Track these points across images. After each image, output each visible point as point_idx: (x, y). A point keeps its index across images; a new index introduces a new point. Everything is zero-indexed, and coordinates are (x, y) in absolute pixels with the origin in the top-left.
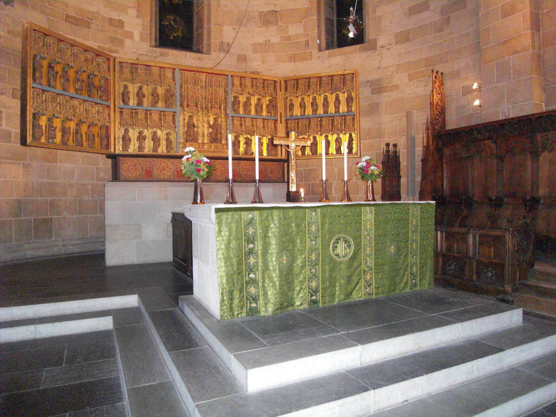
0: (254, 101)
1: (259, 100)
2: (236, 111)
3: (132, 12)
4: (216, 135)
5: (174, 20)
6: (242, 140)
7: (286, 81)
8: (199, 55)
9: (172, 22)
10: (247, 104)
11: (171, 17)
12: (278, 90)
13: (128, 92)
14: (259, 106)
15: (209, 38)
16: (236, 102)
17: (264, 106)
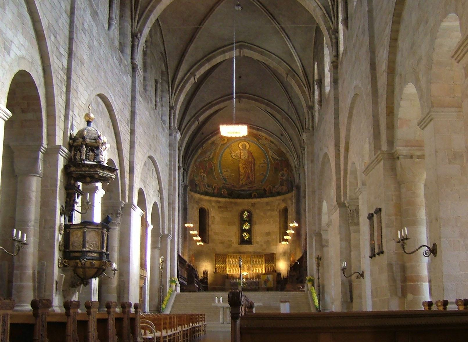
0: (258, 260)
2: (253, 263)
3: (234, 237)
5: (246, 234)
10: (256, 261)
11: (245, 233)
14: (259, 261)
16: (253, 260)
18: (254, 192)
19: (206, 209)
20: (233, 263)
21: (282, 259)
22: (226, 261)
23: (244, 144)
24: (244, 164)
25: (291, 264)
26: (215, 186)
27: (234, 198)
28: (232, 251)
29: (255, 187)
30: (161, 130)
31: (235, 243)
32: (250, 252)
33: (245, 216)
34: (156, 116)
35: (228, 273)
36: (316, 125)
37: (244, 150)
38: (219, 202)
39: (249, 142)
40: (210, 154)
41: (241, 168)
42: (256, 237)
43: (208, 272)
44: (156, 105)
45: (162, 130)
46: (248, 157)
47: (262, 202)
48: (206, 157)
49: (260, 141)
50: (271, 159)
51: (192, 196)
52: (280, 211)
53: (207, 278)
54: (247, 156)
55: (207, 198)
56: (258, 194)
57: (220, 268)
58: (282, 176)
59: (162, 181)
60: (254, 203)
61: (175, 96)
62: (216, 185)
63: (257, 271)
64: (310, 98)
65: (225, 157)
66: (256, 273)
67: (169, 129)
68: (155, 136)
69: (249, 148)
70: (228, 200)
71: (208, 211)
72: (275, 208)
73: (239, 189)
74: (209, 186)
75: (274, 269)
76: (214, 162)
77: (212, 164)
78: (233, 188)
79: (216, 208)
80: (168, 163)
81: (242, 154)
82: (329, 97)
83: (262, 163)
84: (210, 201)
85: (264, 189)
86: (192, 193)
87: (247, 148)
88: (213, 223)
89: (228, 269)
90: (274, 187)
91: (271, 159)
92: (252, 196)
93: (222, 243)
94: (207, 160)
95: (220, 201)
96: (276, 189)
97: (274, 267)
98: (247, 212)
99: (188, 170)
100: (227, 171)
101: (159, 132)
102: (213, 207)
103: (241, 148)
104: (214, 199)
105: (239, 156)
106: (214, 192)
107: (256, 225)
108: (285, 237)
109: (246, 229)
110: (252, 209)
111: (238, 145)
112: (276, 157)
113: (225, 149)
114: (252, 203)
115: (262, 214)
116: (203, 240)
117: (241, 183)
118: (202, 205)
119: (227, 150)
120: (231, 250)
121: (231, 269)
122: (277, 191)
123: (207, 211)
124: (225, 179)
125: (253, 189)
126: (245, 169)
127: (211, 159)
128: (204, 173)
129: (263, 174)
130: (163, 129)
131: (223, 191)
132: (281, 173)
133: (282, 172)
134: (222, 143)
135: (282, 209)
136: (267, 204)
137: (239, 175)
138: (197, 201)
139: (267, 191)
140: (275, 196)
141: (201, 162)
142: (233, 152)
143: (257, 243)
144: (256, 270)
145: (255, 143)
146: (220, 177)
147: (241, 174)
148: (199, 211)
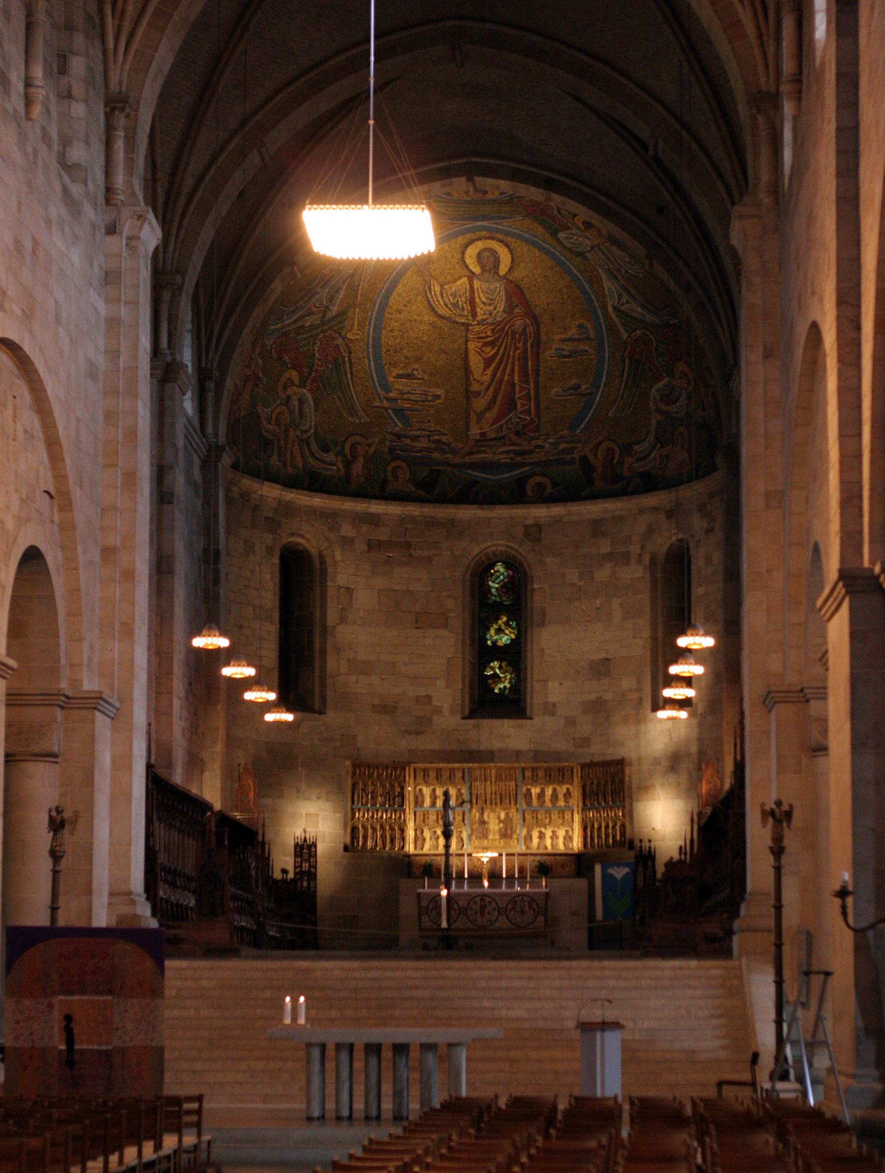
0: (549, 791)
1: (555, 790)
3: (441, 683)
4: (506, 830)
5: (500, 668)
6: (535, 835)
7: (581, 768)
8: (519, 722)
9: (497, 671)
10: (541, 795)
11: (496, 664)
12: (575, 778)
13: (423, 796)
14: (555, 796)
15: (532, 699)
16: (528, 794)
17: (561, 796)
18: (534, 474)
19: (313, 550)
20: (433, 804)
21: (662, 785)
22: (402, 795)
23: (485, 250)
24: (492, 344)
25: (700, 814)
26: (353, 447)
27: (443, 500)
28: (435, 746)
29: (541, 447)
30: (57, 210)
31: (446, 711)
32: (518, 754)
33: (494, 585)
34: (30, 150)
35: (410, 848)
36: (786, 181)
37: (486, 274)
38: (374, 520)
40: (331, 301)
41: (476, 362)
42: (545, 681)
43: (321, 848)
44: (28, 102)
45: (63, 212)
46: (510, 308)
47: (574, 518)
48: (310, 314)
49: (561, 235)
50: (616, 320)
51: (245, 495)
52: (653, 562)
53: (311, 875)
54: (501, 307)
55: (317, 501)
56: (555, 485)
57: (374, 829)
58: (668, 397)
59: (65, 447)
60: (538, 526)
61: (134, 47)
62: (357, 438)
63: (548, 842)
64: (765, 56)
65: (400, 312)
66: (542, 851)
67: (101, 200)
68: (28, 244)
69: (511, 268)
70: (413, 510)
71: (323, 563)
72: (635, 549)
73: (467, 459)
74: (325, 449)
75: (623, 833)
78: (436, 455)
79: (360, 546)
80: (101, 361)
81: (481, 297)
82: (823, 63)
83: (571, 340)
84: (332, 518)
85: (584, 459)
86: (247, 483)
87: (503, 269)
88: (343, 620)
89: (410, 833)
90: (627, 449)
91: (616, 320)
92: (529, 493)
93: (387, 709)
94: (312, 327)
95: (379, 515)
96: (639, 460)
97: (623, 826)
98: (508, 565)
99: (223, 373)
100: (409, 376)
101: (49, 222)
102: (347, 542)
104: (348, 505)
105: (468, 307)
107: (543, 624)
108: (668, 693)
109: (500, 643)
110: (524, 551)
111: (463, 253)
112: (637, 311)
114: (526, 526)
115: (572, 575)
116: (284, 702)
117: (475, 431)
118: (293, 534)
120: (428, 743)
121: (427, 834)
123: (317, 561)
124: (399, 412)
125: (534, 458)
126: (494, 365)
127: (333, 319)
128: (303, 385)
129: (579, 387)
130: (72, 205)
131: (390, 468)
132: (660, 385)
133: (665, 381)
135: (665, 549)
136: (597, 528)
137: (469, 395)
138: (267, 518)
140: (636, 492)
142: (437, 289)
143: (550, 709)
144: (542, 836)
145: (541, 248)
146: (377, 404)
147: (475, 387)
148: (276, 560)
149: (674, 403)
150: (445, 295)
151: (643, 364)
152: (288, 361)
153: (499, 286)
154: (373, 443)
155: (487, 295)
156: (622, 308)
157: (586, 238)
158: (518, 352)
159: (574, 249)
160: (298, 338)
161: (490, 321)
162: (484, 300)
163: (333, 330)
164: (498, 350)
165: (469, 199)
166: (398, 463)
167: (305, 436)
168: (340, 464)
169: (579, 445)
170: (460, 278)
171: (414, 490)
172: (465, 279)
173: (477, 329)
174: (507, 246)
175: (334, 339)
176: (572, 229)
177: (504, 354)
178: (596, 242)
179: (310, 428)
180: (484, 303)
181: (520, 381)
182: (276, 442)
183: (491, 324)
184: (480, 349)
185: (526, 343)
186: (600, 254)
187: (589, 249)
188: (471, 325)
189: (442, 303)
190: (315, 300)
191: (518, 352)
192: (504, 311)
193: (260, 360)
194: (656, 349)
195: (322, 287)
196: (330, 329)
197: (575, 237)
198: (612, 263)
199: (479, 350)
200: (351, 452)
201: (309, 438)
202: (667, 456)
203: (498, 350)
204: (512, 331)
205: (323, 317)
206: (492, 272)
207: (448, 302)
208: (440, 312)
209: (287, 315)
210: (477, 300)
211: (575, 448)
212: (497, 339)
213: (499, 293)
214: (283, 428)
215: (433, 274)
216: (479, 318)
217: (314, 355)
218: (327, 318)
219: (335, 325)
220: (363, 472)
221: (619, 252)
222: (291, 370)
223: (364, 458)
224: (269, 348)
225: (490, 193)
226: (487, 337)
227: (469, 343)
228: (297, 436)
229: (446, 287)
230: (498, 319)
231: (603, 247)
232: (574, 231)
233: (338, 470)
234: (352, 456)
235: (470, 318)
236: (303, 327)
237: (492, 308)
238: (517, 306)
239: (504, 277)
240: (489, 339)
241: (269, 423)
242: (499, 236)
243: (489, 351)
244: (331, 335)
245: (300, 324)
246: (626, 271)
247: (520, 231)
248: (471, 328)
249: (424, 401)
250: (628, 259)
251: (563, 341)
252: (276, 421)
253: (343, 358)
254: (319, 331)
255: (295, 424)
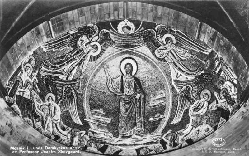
23: (128, 64)
24: (128, 103)
37: (128, 75)
39: (136, 58)
40: (71, 72)
41: (122, 109)
46: (135, 89)
48: (62, 74)
49: (156, 51)
69: (137, 72)
76: (77, 91)
77: (73, 92)
96: (184, 137)
103: (125, 73)
106: (72, 140)
113: (98, 70)
119: (101, 74)
122: (186, 138)
125: (142, 142)
127: (71, 81)
128: (57, 102)
134: (92, 54)
139: (166, 143)
141: (50, 76)
142: (111, 80)
149: (200, 109)
150: (113, 84)
151: (186, 100)
152: (51, 89)
153: (131, 79)
154: (83, 133)
155: (127, 84)
156: (177, 80)
157: (166, 49)
158: (138, 106)
159: (160, 58)
160: (56, 81)
161: (128, 95)
162: (126, 86)
163: (71, 86)
164: (130, 106)
165: (124, 34)
166: (92, 141)
167: (55, 122)
168: (69, 137)
169: (160, 136)
170: (119, 76)
171: (97, 150)
172: (120, 77)
173: (123, 98)
174: (136, 61)
175: (71, 90)
176: (161, 45)
177: (132, 108)
178: (170, 49)
179: (58, 120)
180: (126, 87)
181: (138, 116)
182: (41, 117)
183: (129, 96)
184: (124, 105)
185: (141, 103)
186: (172, 56)
187: (166, 55)
188: (121, 96)
189: (112, 86)
190: (64, 68)
191: (138, 106)
192: (133, 91)
193: (37, 80)
194: (192, 91)
195: (67, 63)
196: (70, 84)
197: (161, 51)
198: (176, 59)
199: (124, 105)
200: (74, 134)
201: (57, 123)
202: (198, 131)
203: (130, 106)
204: (136, 98)
205: (67, 78)
206: (130, 74)
207: (114, 86)
208: (111, 90)
209: (52, 67)
210: (124, 86)
211: (158, 138)
212: (130, 102)
213: (132, 83)
214: (46, 114)
215: (109, 73)
216: (124, 93)
217: (62, 93)
218: (68, 79)
219: (72, 84)
220: (78, 141)
221: (179, 50)
222: (51, 93)
223: (79, 137)
224: (42, 77)
225: (131, 29)
226: (127, 101)
227: (121, 103)
228: (52, 120)
229: (113, 80)
230: (131, 94)
231: (173, 51)
232: (161, 47)
233: (68, 138)
234: (74, 135)
235: (121, 93)
236: (58, 77)
237: (129, 90)
238: (138, 88)
239: (134, 76)
240: (127, 102)
241: (40, 109)
242: (133, 57)
243: (127, 106)
244: (70, 87)
245: (57, 75)
246: (181, 59)
247: (141, 53)
248: (121, 97)
249: (103, 122)
250: (183, 52)
251: (154, 100)
252: (43, 110)
253: (74, 99)
254: (65, 83)
255: (51, 115)
